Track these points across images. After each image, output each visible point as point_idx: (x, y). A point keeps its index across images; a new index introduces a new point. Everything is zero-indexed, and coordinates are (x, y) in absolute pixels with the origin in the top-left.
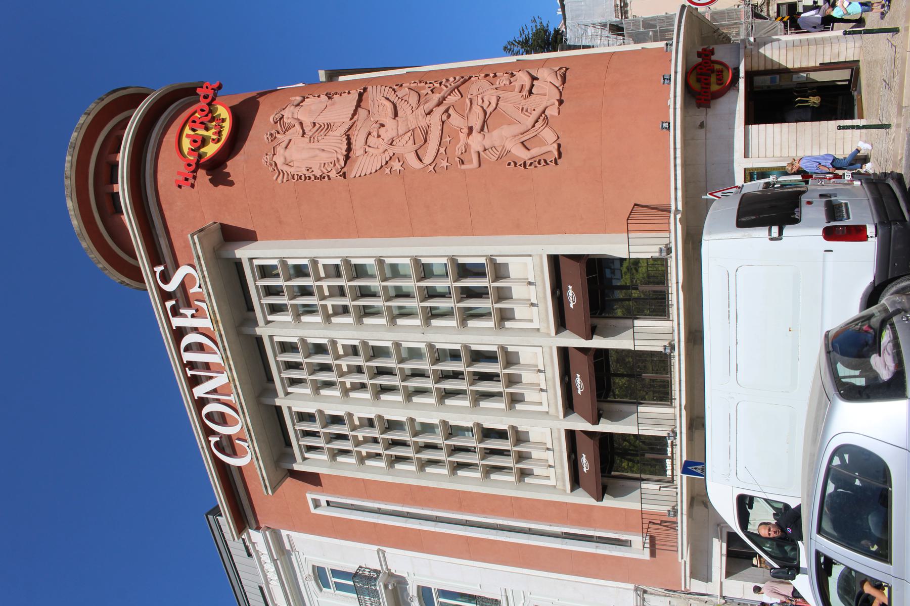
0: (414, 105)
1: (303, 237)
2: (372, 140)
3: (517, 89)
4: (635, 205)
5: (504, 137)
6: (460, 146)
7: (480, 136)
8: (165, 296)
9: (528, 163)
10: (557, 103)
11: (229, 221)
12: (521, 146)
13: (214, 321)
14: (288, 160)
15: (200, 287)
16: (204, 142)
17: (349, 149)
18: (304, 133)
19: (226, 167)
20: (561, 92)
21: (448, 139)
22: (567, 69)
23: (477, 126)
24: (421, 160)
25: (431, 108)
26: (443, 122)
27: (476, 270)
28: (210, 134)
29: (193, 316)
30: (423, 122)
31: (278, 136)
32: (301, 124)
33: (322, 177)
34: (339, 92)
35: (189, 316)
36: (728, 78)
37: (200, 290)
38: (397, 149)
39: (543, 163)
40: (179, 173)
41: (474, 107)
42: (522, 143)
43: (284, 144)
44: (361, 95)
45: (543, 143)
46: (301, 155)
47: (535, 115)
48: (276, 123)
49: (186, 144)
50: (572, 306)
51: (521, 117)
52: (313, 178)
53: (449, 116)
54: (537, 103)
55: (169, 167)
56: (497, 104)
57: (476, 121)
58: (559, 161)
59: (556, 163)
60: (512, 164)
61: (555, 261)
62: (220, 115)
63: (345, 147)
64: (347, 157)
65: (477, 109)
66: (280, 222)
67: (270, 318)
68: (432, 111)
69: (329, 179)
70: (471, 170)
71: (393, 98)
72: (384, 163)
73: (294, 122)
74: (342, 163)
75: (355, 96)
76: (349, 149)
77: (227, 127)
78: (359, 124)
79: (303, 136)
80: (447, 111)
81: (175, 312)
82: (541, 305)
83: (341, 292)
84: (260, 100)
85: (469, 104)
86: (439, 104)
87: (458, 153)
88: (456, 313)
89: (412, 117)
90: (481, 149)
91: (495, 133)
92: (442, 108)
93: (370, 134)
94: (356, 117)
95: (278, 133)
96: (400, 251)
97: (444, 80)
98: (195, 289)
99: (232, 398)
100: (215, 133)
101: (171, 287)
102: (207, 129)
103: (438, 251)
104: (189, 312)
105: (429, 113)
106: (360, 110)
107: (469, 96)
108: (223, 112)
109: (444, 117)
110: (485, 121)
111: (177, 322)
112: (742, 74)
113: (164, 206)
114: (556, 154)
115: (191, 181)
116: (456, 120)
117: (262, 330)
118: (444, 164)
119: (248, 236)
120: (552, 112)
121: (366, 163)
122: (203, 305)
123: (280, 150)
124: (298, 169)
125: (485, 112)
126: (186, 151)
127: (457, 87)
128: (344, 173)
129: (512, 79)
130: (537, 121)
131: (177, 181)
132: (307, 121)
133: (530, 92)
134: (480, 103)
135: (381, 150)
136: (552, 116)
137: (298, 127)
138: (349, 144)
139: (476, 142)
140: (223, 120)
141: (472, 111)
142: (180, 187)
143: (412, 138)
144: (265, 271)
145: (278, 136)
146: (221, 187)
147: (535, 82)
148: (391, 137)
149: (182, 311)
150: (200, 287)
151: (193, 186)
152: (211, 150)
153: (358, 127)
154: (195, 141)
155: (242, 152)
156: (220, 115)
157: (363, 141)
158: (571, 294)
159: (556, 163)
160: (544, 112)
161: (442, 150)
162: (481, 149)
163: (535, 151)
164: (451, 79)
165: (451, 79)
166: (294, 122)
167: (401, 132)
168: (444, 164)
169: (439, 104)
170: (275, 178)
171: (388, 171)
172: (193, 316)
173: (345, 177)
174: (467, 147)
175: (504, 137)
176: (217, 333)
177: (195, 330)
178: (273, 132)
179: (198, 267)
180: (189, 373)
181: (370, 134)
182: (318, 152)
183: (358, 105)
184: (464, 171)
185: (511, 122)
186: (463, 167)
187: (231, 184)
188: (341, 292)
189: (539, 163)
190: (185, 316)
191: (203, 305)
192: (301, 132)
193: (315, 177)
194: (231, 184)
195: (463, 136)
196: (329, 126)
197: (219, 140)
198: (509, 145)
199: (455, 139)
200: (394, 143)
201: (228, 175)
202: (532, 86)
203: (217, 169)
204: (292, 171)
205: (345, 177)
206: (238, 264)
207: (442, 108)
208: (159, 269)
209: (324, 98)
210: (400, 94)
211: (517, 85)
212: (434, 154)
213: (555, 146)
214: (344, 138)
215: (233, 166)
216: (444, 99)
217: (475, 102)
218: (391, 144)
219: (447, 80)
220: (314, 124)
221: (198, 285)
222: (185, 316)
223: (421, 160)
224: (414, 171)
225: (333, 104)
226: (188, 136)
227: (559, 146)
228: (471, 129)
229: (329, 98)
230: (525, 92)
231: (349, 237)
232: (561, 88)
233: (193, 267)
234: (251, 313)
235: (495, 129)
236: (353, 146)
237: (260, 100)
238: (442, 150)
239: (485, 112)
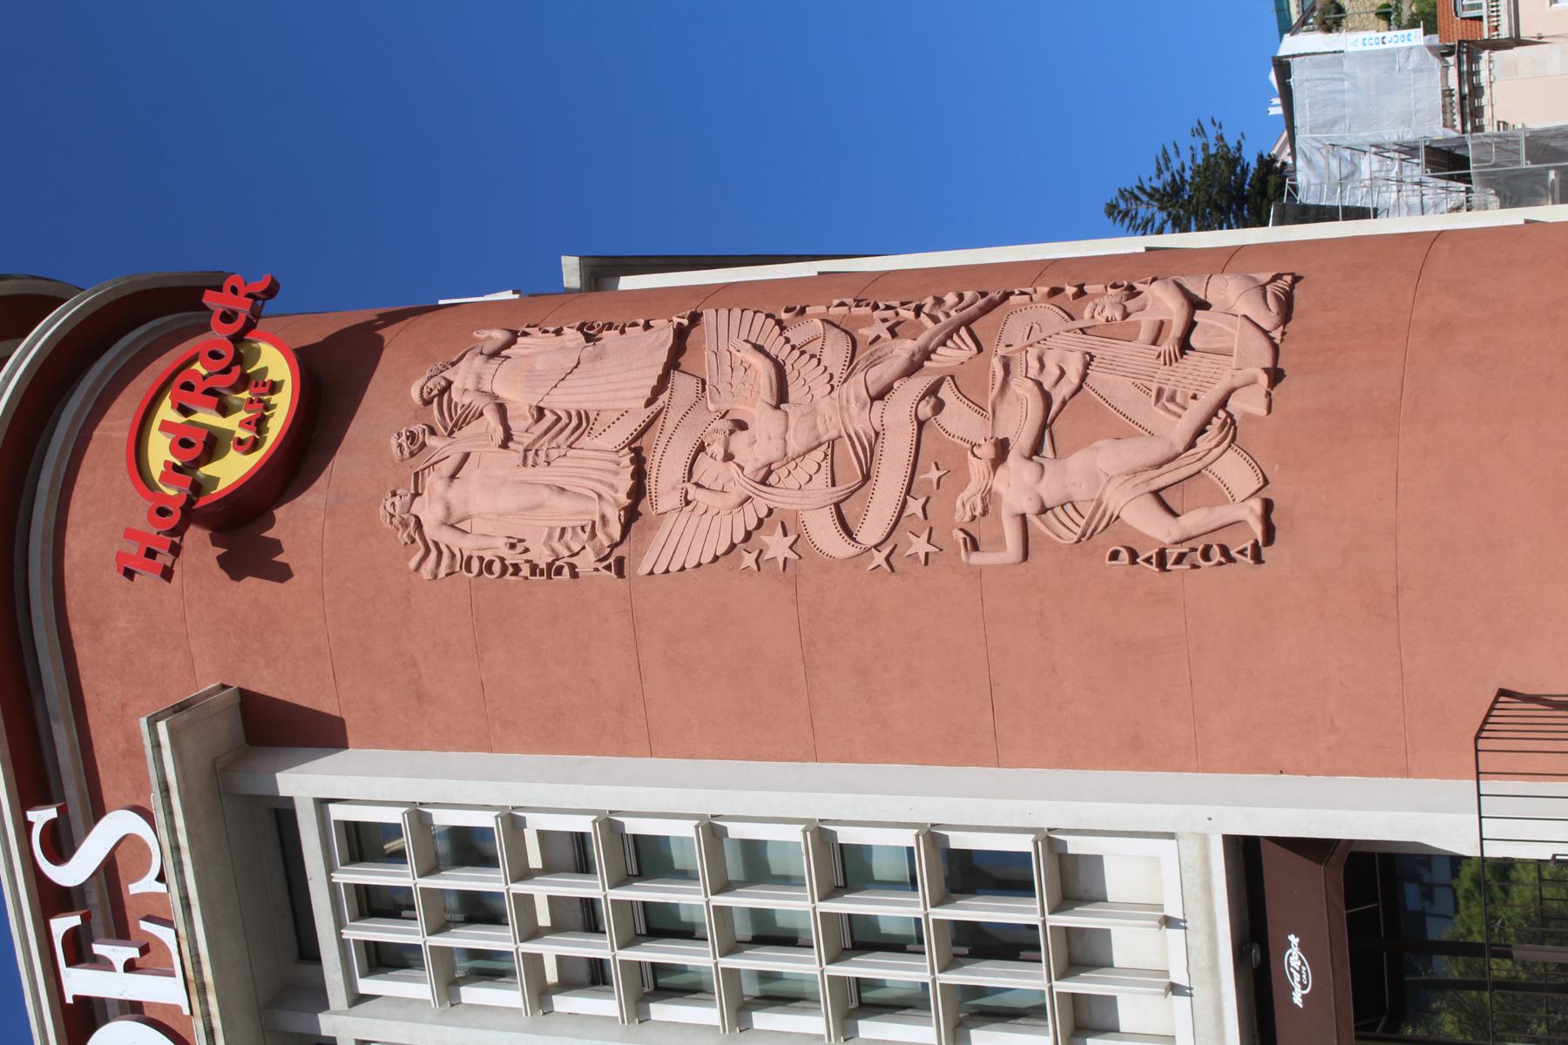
0: (838, 369)
1: (484, 742)
2: (708, 468)
3: (1145, 334)
4: (1502, 692)
5: (1101, 476)
6: (970, 496)
7: (1028, 471)
8: (51, 899)
9: (1172, 553)
10: (1263, 379)
11: (267, 684)
12: (1150, 497)
13: (194, 986)
14: (457, 513)
15: (161, 878)
16: (213, 445)
17: (638, 491)
18: (508, 438)
19: (271, 523)
20: (1276, 349)
21: (934, 474)
22: (1296, 279)
23: (1022, 440)
24: (849, 533)
25: (886, 379)
26: (921, 425)
27: (1001, 873)
28: (231, 424)
29: (130, 966)
30: (861, 422)
31: (432, 441)
32: (502, 409)
33: (553, 570)
34: (618, 322)
35: (119, 966)
37: (161, 888)
38: (781, 498)
39: (1216, 555)
40: (130, 534)
41: (1013, 383)
42: (1156, 494)
43: (446, 467)
44: (681, 334)
45: (1219, 496)
46: (493, 501)
47: (1196, 412)
48: (428, 402)
49: (160, 451)
50: (1297, 999)
51: (1153, 416)
52: (526, 570)
53: (939, 406)
54: (1203, 377)
55: (100, 514)
56: (1084, 377)
57: (1020, 423)
58: (1266, 553)
59: (1257, 558)
60: (1124, 555)
61: (1247, 857)
62: (265, 371)
63: (625, 482)
64: (631, 515)
65: (1022, 389)
66: (420, 697)
67: (366, 986)
68: (888, 389)
69: (574, 575)
70: (999, 568)
71: (776, 347)
72: (739, 536)
73: (480, 402)
74: (616, 530)
75: (663, 334)
76: (638, 491)
77: (283, 405)
78: (673, 417)
79: (504, 445)
80: (933, 390)
81: (79, 951)
82: (1202, 992)
83: (587, 917)
84: (387, 333)
85: (1000, 373)
86: (913, 368)
87: (962, 516)
88: (936, 1001)
89: (829, 404)
90: (1030, 508)
91: (1076, 462)
92: (920, 383)
93: (701, 448)
94: (664, 397)
95: (433, 432)
96: (776, 802)
97: (929, 301)
98: (145, 885)
100: (245, 424)
101: (71, 874)
102: (224, 410)
103: (886, 807)
104: (119, 954)
105: (880, 396)
106: (677, 378)
107: (1002, 351)
108: (274, 362)
109: (925, 410)
110: (1045, 426)
111: (79, 982)
113: (76, 629)
114: (1258, 529)
115: (164, 558)
116: (958, 419)
118: (920, 546)
119: (320, 733)
120: (1249, 404)
121: (684, 536)
122: (166, 935)
123: (434, 482)
124: (483, 542)
125: (1047, 399)
126: (156, 468)
127: (967, 323)
128: (620, 561)
129: (1131, 305)
130: (1201, 431)
131: (121, 556)
132: (520, 401)
133: (1184, 345)
134: (1033, 373)
135: (734, 498)
136: (1249, 417)
137: (491, 417)
138: (639, 475)
139: (1017, 486)
140: (275, 387)
141: (1009, 395)
142: (129, 574)
143: (826, 465)
144: (363, 842)
145: (432, 441)
146: (251, 582)
147: (1200, 316)
148: (763, 460)
149: (98, 949)
150: (161, 878)
151: (167, 574)
152: (230, 470)
153: (669, 426)
154: (185, 443)
155: (321, 481)
156: (265, 371)
157: (681, 470)
158: (1295, 962)
159: (1257, 558)
160: (1223, 404)
161: (914, 506)
162: (1030, 508)
163: (1195, 520)
164: (951, 298)
165: (951, 298)
166: (480, 402)
167: (794, 447)
168: (920, 546)
170: (413, 563)
171: (749, 560)
172: (130, 966)
173: (620, 574)
174: (989, 499)
175: (1101, 476)
176: (198, 1025)
177: (134, 1010)
178: (418, 428)
179: (160, 818)
181: (701, 448)
182: (545, 493)
183: (673, 363)
184: (979, 572)
185: (1126, 430)
186: (976, 558)
187: (282, 574)
188: (587, 917)
189: (1206, 555)
190: (105, 964)
191: (166, 935)
192: (499, 434)
193: (534, 569)
194: (282, 574)
195: (977, 468)
196: (583, 422)
197: (255, 445)
198: (1116, 500)
199: (956, 475)
200: (773, 479)
201: (276, 546)
202: (1191, 325)
203: (242, 530)
204: (467, 545)
205: (620, 574)
206: (283, 815)
207: (920, 383)
208: (40, 817)
209: (572, 336)
210: (797, 335)
211: (1145, 322)
212: (889, 515)
213: (1256, 505)
214: (626, 459)
215: (295, 524)
216: (927, 354)
217: (1017, 369)
218: (763, 482)
219: (939, 301)
220: (541, 412)
221: (155, 870)
222: (105, 964)
223: (849, 533)
224: (829, 564)
225: (599, 357)
226: (166, 427)
227: (1268, 506)
228: (1002, 448)
229: (589, 338)
230: (1169, 344)
231: (622, 753)
232: (1277, 335)
233: (148, 816)
234: (310, 967)
235: (1075, 448)
236: (650, 484)
237: (387, 333)
238: (914, 506)
239: (1047, 399)
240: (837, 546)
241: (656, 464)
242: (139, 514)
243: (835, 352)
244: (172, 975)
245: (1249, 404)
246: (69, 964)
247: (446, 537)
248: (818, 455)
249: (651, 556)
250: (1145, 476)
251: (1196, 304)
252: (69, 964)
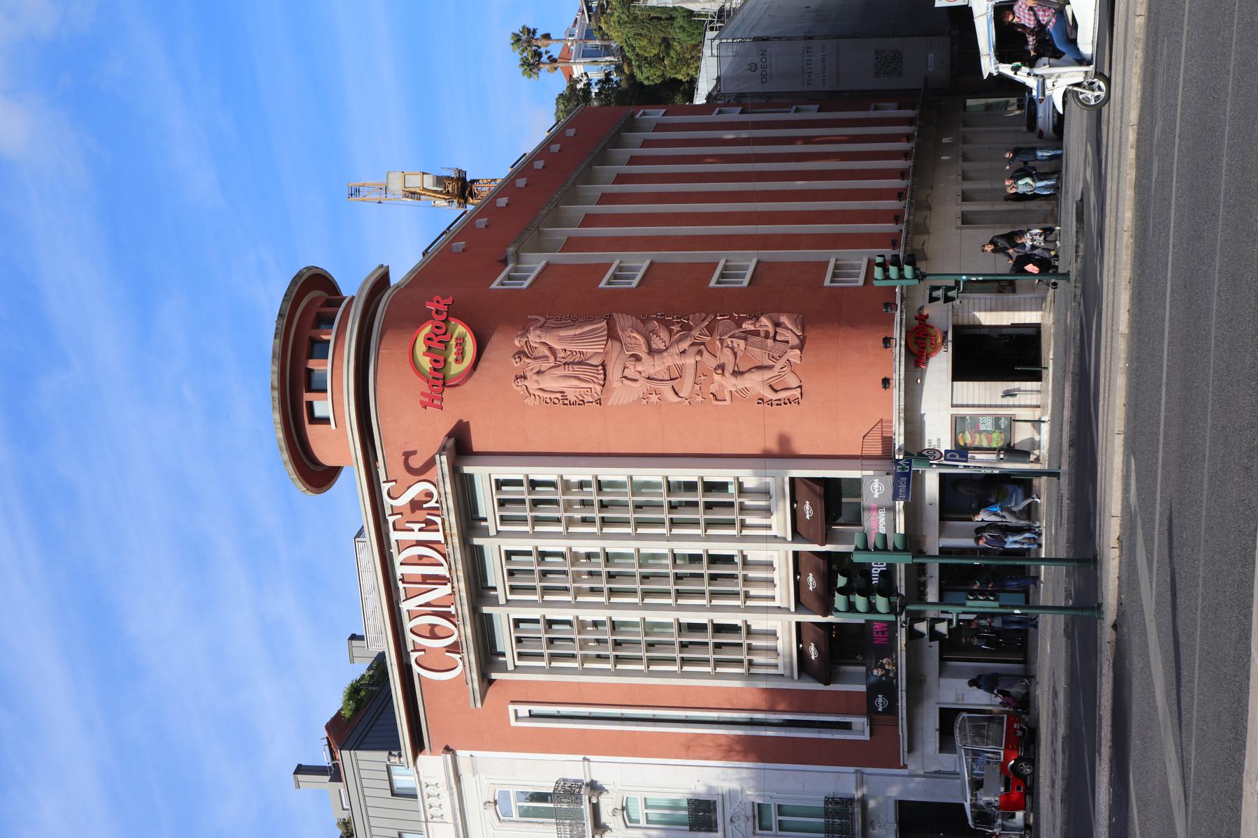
29: (420, 530)
30: (679, 362)
40: (423, 394)
90: (733, 389)
98: (432, 504)
99: (452, 610)
104: (416, 527)
122: (438, 520)
147: (778, 330)
168: (699, 399)
172: (420, 530)
221: (435, 499)
240: (675, 399)
242: (425, 387)
247: (537, 393)
251: (777, 324)
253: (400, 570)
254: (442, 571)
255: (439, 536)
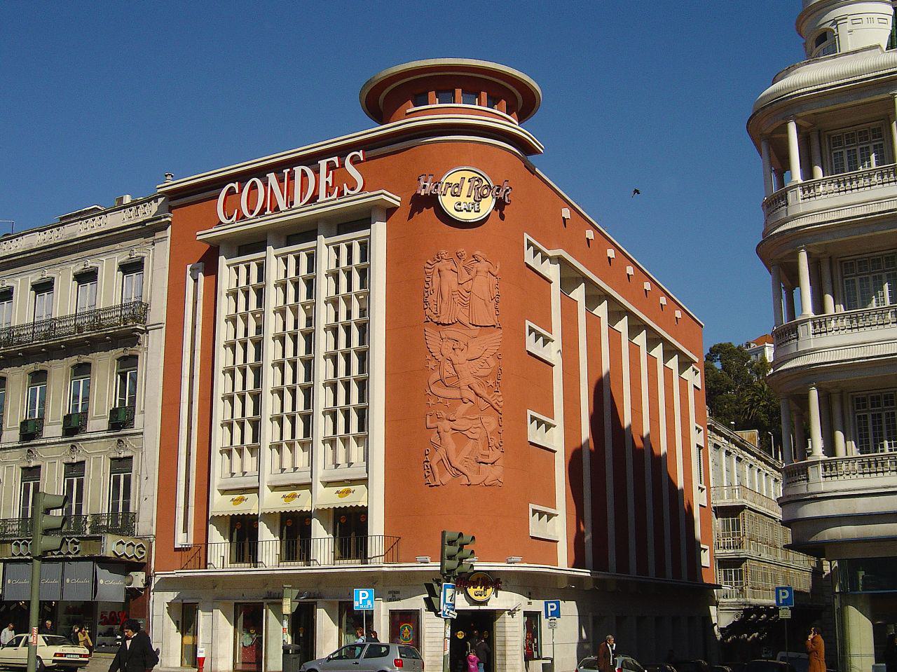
0: (478, 374)
3: (486, 452)
15: (348, 194)
27: (361, 424)
29: (327, 182)
30: (463, 384)
35: (327, 180)
36: (478, 598)
43: (455, 268)
48: (473, 256)
73: (473, 273)
76: (444, 325)
81: (330, 167)
92: (473, 397)
98: (346, 190)
99: (268, 212)
104: (330, 179)
112: (482, 608)
117: (321, 239)
122: (335, 196)
123: (451, 265)
128: (428, 321)
150: (348, 194)
153: (462, 331)
161: (441, 400)
163: (435, 468)
165: (501, 399)
169: (477, 394)
171: (429, 357)
172: (327, 182)
180: (286, 171)
185: (458, 451)
191: (335, 196)
198: (441, 451)
202: (487, 464)
230: (480, 459)
238: (441, 400)
241: (452, 329)
243: (482, 372)
244: (327, 197)
245: (465, 481)
246: (328, 162)
248: (454, 373)
249: (430, 331)
250: (445, 455)
252: (328, 162)
253: (298, 170)
254: (297, 203)
255: (322, 197)
